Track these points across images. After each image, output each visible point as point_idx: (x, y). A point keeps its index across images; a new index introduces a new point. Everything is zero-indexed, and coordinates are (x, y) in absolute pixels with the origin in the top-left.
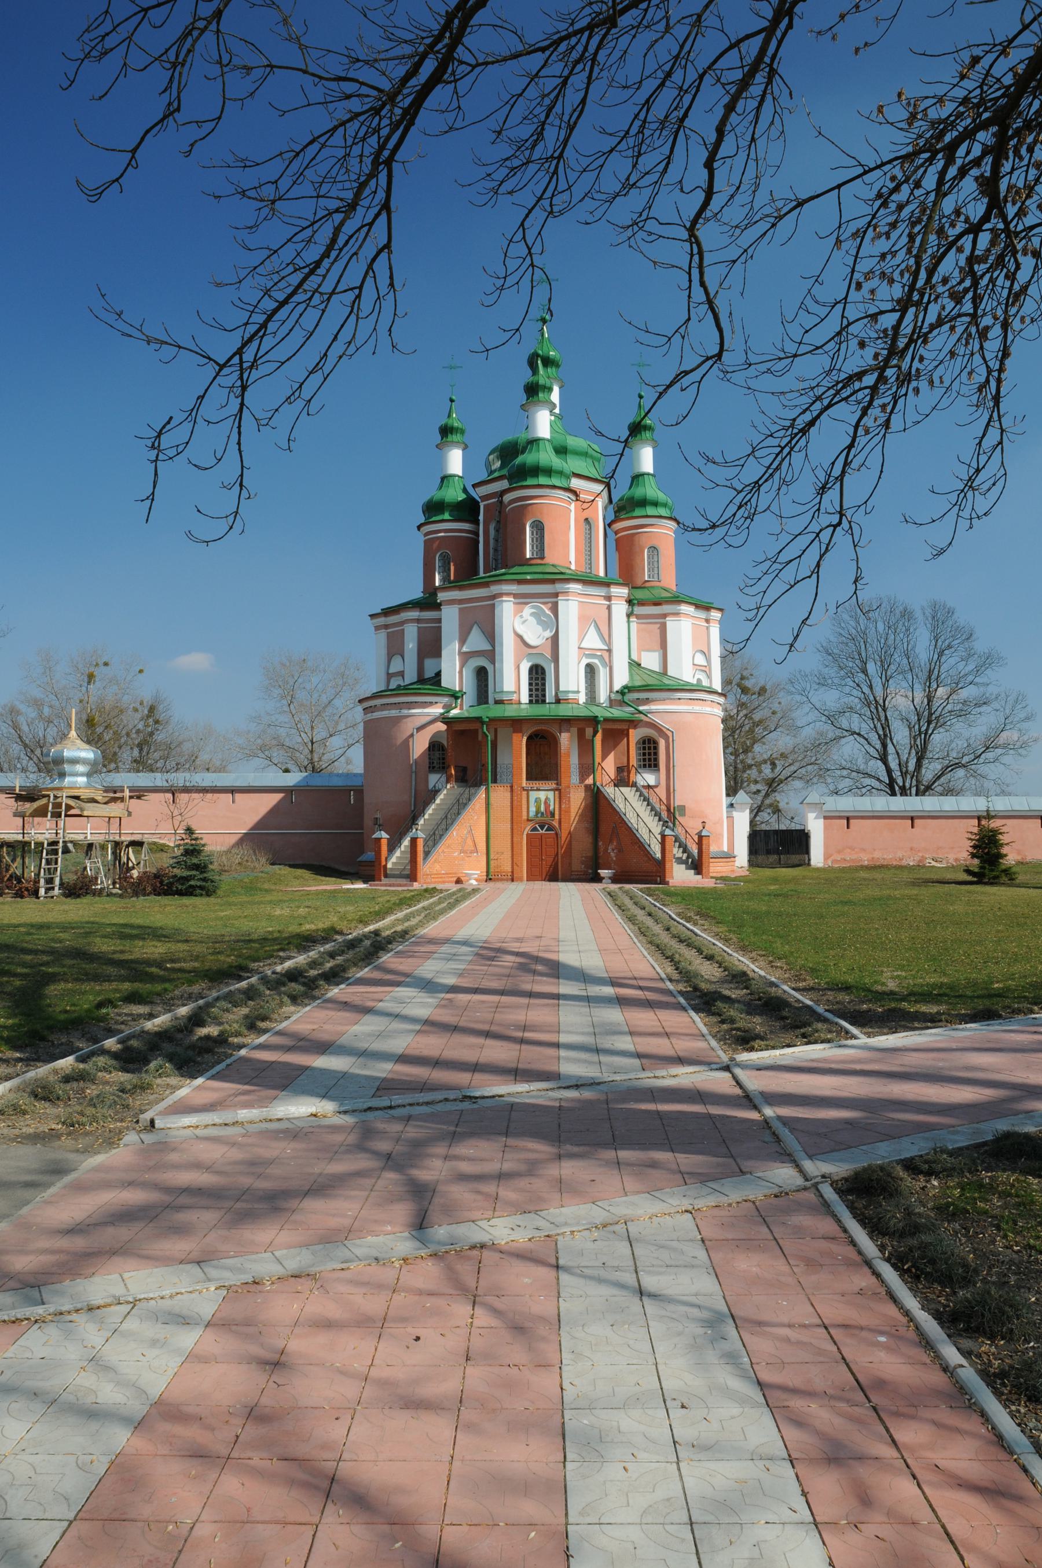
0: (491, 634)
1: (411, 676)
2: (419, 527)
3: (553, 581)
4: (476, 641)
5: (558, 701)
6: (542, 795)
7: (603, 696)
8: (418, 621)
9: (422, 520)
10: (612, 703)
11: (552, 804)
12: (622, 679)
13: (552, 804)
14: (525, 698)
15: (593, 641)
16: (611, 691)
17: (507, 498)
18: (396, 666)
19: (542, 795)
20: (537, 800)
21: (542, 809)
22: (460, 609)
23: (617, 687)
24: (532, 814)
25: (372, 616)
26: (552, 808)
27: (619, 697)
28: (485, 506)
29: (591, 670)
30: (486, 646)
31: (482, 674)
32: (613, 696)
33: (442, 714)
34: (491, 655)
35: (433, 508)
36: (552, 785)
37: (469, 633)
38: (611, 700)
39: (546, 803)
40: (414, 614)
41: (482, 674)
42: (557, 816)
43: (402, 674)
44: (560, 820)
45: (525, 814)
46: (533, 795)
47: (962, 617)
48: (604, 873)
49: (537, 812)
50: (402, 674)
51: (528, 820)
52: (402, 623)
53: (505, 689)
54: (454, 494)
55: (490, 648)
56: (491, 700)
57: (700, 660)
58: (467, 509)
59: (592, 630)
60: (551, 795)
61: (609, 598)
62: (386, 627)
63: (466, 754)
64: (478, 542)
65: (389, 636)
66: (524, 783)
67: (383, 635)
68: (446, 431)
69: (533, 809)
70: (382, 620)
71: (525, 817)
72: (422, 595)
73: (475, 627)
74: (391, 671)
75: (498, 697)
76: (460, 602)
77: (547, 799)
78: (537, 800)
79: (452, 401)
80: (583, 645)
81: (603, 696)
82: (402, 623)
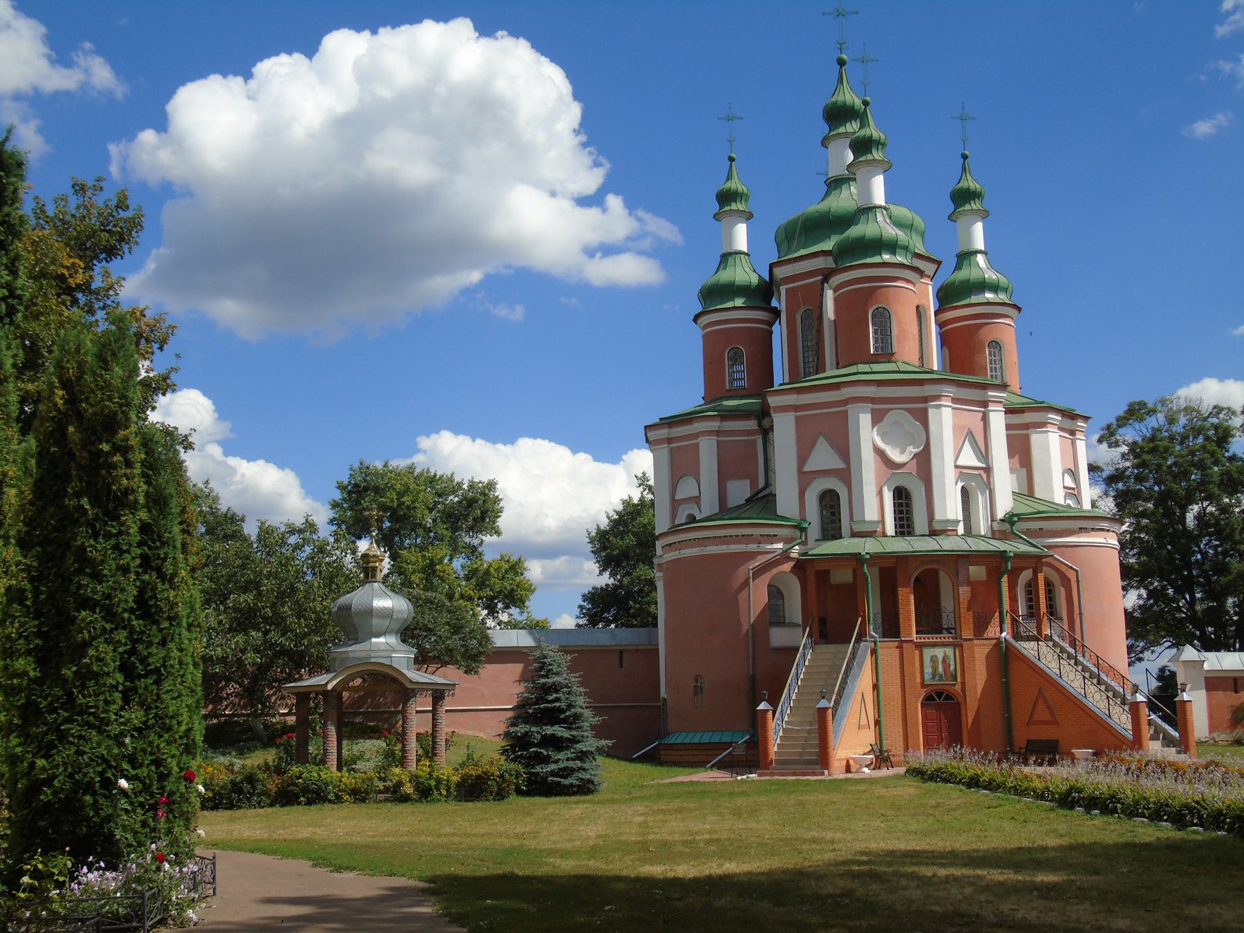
0: (844, 446)
1: (709, 505)
2: (696, 319)
4: (823, 457)
5: (933, 533)
6: (939, 652)
7: (983, 527)
8: (718, 433)
9: (699, 309)
10: (995, 535)
11: (952, 663)
12: (1004, 505)
14: (890, 528)
15: (969, 458)
17: (837, 280)
18: (687, 489)
19: (939, 653)
20: (934, 660)
21: (940, 669)
22: (797, 418)
23: (1000, 515)
26: (952, 668)
27: (1007, 526)
28: (787, 290)
31: (829, 502)
32: (996, 526)
34: (846, 475)
35: (714, 294)
36: (946, 637)
37: (813, 444)
38: (993, 532)
39: (944, 661)
41: (829, 502)
42: (959, 680)
43: (696, 500)
44: (963, 683)
46: (928, 653)
49: (934, 675)
50: (696, 500)
52: (697, 435)
53: (867, 518)
54: (744, 274)
55: (842, 465)
56: (845, 529)
57: (1069, 482)
58: (762, 293)
59: (967, 446)
60: (949, 651)
61: (984, 404)
62: (669, 440)
63: (841, 601)
64: (771, 333)
66: (914, 636)
67: (664, 450)
68: (726, 197)
69: (928, 670)
70: (663, 433)
75: (857, 528)
76: (796, 408)
78: (934, 660)
79: (731, 159)
80: (960, 463)
81: (983, 527)
82: (697, 435)
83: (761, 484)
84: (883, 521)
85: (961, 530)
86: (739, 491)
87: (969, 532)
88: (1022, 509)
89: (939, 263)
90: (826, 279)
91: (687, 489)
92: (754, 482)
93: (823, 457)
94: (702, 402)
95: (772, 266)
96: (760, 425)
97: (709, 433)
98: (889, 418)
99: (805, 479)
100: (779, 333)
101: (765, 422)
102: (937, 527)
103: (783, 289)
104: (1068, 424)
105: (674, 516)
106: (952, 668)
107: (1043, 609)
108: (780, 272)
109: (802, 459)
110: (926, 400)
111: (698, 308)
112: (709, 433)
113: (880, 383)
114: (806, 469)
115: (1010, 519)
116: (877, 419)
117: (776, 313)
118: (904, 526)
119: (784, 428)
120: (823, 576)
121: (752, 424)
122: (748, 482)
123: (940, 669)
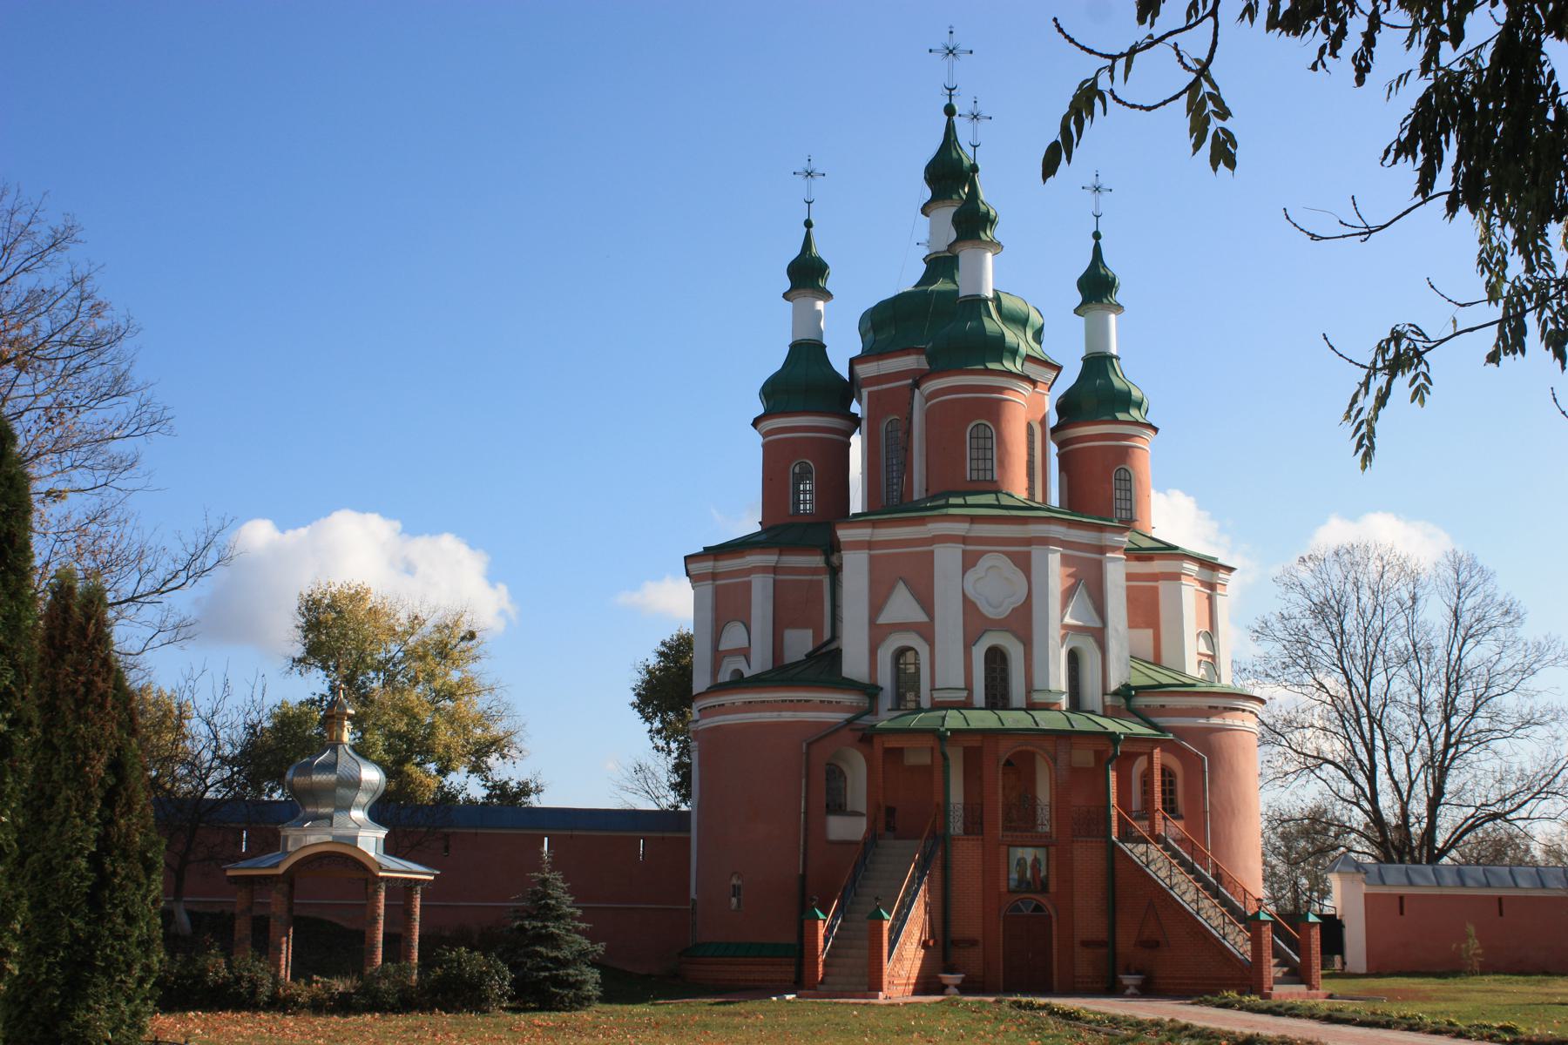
2: (755, 423)
3: (1024, 521)
4: (902, 606)
5: (1031, 707)
6: (1028, 854)
8: (775, 570)
11: (1043, 868)
13: (1043, 868)
16: (1105, 693)
21: (1028, 875)
22: (872, 558)
23: (1114, 685)
24: (1013, 884)
25: (688, 559)
26: (1043, 874)
29: (1074, 658)
30: (919, 616)
33: (849, 722)
34: (926, 632)
40: (770, 559)
43: (745, 653)
45: (1003, 884)
47: (1505, 586)
48: (1129, 980)
49: (1022, 879)
50: (745, 653)
51: (1009, 891)
60: (1041, 854)
62: (714, 576)
65: (718, 594)
67: (708, 587)
69: (1014, 875)
70: (707, 566)
71: (1004, 889)
72: (758, 528)
73: (901, 585)
74: (722, 647)
76: (870, 545)
77: (1036, 860)
78: (1021, 862)
83: (827, 635)
84: (969, 688)
85: (1064, 702)
86: (800, 643)
87: (1076, 704)
88: (1138, 680)
89: (1059, 369)
90: (917, 385)
91: (734, 636)
92: (818, 633)
93: (902, 606)
94: (758, 528)
95: (853, 362)
96: (828, 562)
97: (764, 570)
98: (984, 563)
99: (878, 634)
100: (856, 443)
101: (834, 559)
102: (1038, 698)
103: (865, 392)
104: (1206, 575)
105: (715, 669)
106: (1043, 874)
107: (1158, 804)
108: (865, 370)
109: (876, 608)
110: (1029, 542)
111: (760, 410)
112: (764, 570)
113: (973, 519)
114: (882, 620)
115: (1126, 691)
116: (969, 562)
117: (855, 421)
118: (997, 697)
119: (855, 567)
120: (895, 754)
121: (817, 561)
122: (810, 632)
123: (1028, 875)
